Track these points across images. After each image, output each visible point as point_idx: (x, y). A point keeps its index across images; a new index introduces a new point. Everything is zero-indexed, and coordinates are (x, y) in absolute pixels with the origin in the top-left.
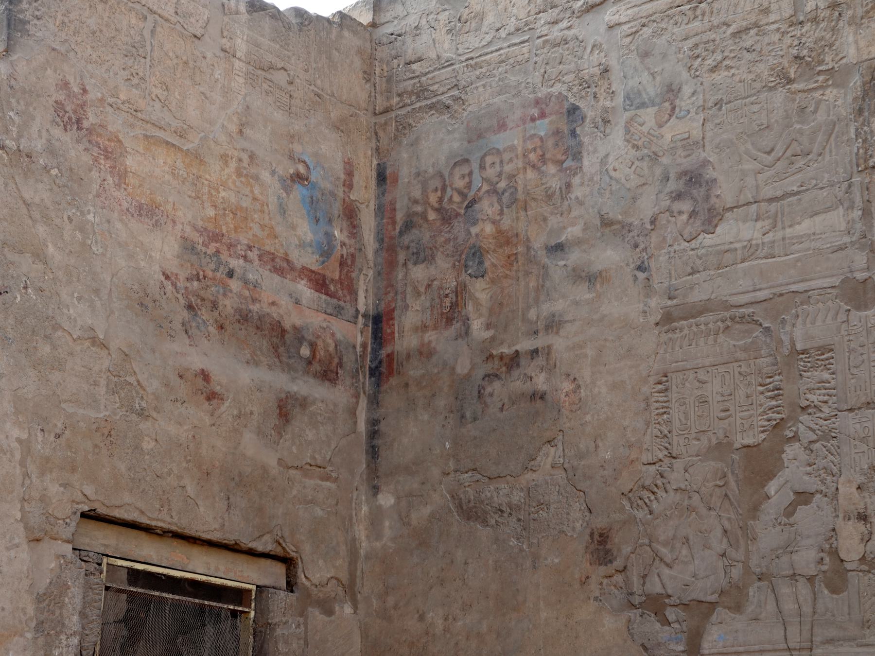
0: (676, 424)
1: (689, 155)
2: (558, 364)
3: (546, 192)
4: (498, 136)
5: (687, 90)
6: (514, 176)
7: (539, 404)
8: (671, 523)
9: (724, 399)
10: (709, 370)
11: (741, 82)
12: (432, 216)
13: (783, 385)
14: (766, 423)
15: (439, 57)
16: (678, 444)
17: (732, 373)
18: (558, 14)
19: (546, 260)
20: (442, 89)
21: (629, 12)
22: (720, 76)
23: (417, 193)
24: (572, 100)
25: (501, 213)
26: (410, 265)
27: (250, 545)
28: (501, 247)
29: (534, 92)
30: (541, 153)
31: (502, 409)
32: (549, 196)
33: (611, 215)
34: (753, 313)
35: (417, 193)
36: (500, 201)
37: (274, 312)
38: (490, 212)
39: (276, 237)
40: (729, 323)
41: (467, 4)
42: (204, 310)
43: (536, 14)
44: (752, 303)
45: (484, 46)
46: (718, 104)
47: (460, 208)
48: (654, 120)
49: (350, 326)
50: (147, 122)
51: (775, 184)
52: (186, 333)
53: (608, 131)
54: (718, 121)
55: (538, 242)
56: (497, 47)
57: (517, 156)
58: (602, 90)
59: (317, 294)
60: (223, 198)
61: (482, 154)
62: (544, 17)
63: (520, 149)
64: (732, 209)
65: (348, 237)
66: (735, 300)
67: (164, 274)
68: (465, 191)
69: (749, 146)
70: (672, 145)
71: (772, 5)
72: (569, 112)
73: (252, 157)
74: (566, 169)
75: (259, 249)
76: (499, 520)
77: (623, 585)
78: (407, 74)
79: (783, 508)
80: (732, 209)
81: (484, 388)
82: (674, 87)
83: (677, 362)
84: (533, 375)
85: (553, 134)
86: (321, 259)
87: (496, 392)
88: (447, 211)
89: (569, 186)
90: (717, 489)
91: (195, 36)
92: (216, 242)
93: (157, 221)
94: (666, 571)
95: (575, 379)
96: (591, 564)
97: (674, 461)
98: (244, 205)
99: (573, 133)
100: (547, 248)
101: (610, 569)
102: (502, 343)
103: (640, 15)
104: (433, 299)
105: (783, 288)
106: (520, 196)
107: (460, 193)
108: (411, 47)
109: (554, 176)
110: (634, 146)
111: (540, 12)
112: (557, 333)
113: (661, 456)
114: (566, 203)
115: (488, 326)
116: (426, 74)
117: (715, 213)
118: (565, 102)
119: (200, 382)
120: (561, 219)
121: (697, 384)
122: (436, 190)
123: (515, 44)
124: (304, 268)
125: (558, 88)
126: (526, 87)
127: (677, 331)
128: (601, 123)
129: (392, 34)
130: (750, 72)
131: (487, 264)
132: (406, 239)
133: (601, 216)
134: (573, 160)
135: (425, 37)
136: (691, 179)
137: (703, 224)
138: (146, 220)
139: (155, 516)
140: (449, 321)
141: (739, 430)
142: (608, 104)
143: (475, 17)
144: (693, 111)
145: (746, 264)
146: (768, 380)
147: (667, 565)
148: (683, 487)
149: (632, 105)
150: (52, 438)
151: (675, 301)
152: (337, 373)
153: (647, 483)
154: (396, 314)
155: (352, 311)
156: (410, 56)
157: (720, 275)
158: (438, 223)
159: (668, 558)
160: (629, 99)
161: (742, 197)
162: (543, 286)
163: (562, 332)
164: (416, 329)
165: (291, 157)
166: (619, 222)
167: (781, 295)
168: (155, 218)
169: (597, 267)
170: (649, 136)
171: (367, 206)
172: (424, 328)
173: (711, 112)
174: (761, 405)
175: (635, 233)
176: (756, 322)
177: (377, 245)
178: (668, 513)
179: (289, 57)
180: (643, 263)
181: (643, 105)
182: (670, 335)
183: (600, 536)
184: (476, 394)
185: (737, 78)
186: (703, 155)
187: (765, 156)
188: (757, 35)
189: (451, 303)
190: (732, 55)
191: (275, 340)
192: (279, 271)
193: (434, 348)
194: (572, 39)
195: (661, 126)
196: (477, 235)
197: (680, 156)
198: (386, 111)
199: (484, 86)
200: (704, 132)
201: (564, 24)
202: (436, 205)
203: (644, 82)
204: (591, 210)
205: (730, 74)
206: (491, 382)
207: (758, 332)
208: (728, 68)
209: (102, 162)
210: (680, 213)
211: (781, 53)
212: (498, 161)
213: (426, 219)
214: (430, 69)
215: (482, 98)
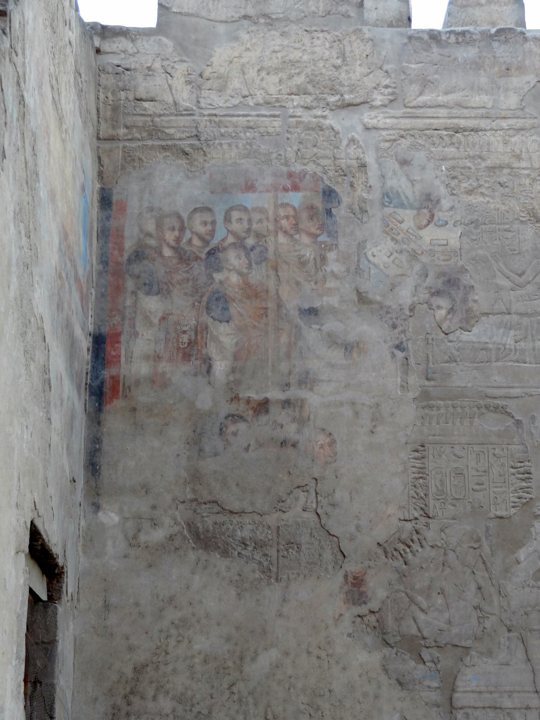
0: (433, 490)
1: (447, 260)
2: (312, 417)
3: (300, 259)
4: (245, 195)
5: (446, 203)
6: (265, 236)
7: (290, 451)
8: (427, 574)
9: (479, 474)
10: (466, 447)
11: (495, 210)
12: (167, 252)
13: (533, 470)
14: (518, 500)
15: (175, 104)
16: (435, 506)
17: (486, 453)
18: (312, 102)
19: (299, 320)
20: (178, 135)
21: (388, 121)
22: (476, 199)
23: (151, 227)
24: (328, 182)
25: (250, 266)
26: (141, 295)
28: (249, 297)
29: (286, 164)
30: (294, 222)
31: (247, 449)
32: (302, 263)
33: (370, 296)
34: (506, 405)
35: (151, 227)
36: (247, 255)
40: (483, 410)
41: (209, 63)
43: (288, 94)
44: (506, 397)
45: (228, 108)
46: (475, 223)
47: (200, 252)
48: (413, 221)
51: (526, 302)
53: (365, 219)
54: (474, 237)
55: (292, 302)
56: (245, 113)
57: (267, 219)
58: (360, 182)
61: (227, 207)
62: (297, 100)
64: (487, 314)
66: (489, 391)
68: (208, 237)
69: (503, 266)
70: (431, 248)
71: (523, 154)
72: (324, 192)
74: (321, 243)
76: (243, 552)
77: (376, 624)
78: (138, 109)
79: (531, 572)
80: (487, 314)
81: (226, 427)
82: (432, 197)
83: (434, 435)
84: (284, 423)
85: (307, 208)
87: (240, 432)
88: (185, 252)
89: (324, 259)
90: (471, 550)
94: (421, 616)
95: (330, 434)
96: (344, 603)
97: (430, 521)
99: (329, 212)
100: (300, 309)
101: (363, 610)
102: (249, 388)
103: (399, 127)
104: (168, 333)
105: (533, 390)
106: (270, 254)
108: (143, 88)
109: (307, 246)
110: (393, 239)
111: (292, 94)
112: (311, 389)
113: (416, 515)
114: (320, 274)
115: (233, 370)
116: (160, 115)
117: (472, 315)
118: (320, 183)
120: (315, 287)
121: (454, 457)
122: (173, 229)
123: (265, 116)
125: (311, 168)
126: (277, 158)
127: (435, 409)
128: (358, 211)
129: (118, 66)
130: (504, 204)
132: (136, 268)
133: (359, 293)
134: (329, 236)
135: (160, 80)
136: (449, 281)
137: (461, 321)
140: (187, 357)
141: (492, 502)
142: (365, 195)
143: (218, 78)
144: (451, 223)
145: (500, 364)
146: (519, 465)
147: (422, 610)
148: (440, 545)
149: (390, 203)
151: (433, 383)
153: (404, 536)
154: (123, 338)
156: (141, 92)
157: (477, 368)
158: (175, 261)
159: (424, 605)
160: (388, 197)
161: (496, 306)
162: (295, 344)
163: (315, 388)
164: (147, 358)
166: (378, 303)
167: (532, 395)
169: (352, 338)
170: (408, 234)
172: (158, 358)
173: (467, 228)
174: (512, 484)
175: (394, 315)
176: (509, 414)
177: (101, 267)
178: (424, 566)
180: (401, 343)
181: (402, 206)
182: (427, 411)
183: (354, 579)
184: (217, 430)
185: (492, 206)
186: (460, 263)
187: (517, 277)
188: (509, 174)
189: (190, 340)
190: (487, 185)
193: (169, 379)
194: (327, 128)
195: (420, 228)
196: (221, 282)
197: (438, 258)
198: (112, 139)
199: (230, 145)
200: (461, 243)
201: (319, 112)
202: (173, 244)
203: (404, 186)
204: (347, 285)
205: (485, 201)
206: (234, 422)
207: (510, 422)
208: (482, 194)
210: (439, 307)
211: (532, 196)
212: (245, 217)
213: (161, 254)
214: (165, 111)
215: (224, 156)
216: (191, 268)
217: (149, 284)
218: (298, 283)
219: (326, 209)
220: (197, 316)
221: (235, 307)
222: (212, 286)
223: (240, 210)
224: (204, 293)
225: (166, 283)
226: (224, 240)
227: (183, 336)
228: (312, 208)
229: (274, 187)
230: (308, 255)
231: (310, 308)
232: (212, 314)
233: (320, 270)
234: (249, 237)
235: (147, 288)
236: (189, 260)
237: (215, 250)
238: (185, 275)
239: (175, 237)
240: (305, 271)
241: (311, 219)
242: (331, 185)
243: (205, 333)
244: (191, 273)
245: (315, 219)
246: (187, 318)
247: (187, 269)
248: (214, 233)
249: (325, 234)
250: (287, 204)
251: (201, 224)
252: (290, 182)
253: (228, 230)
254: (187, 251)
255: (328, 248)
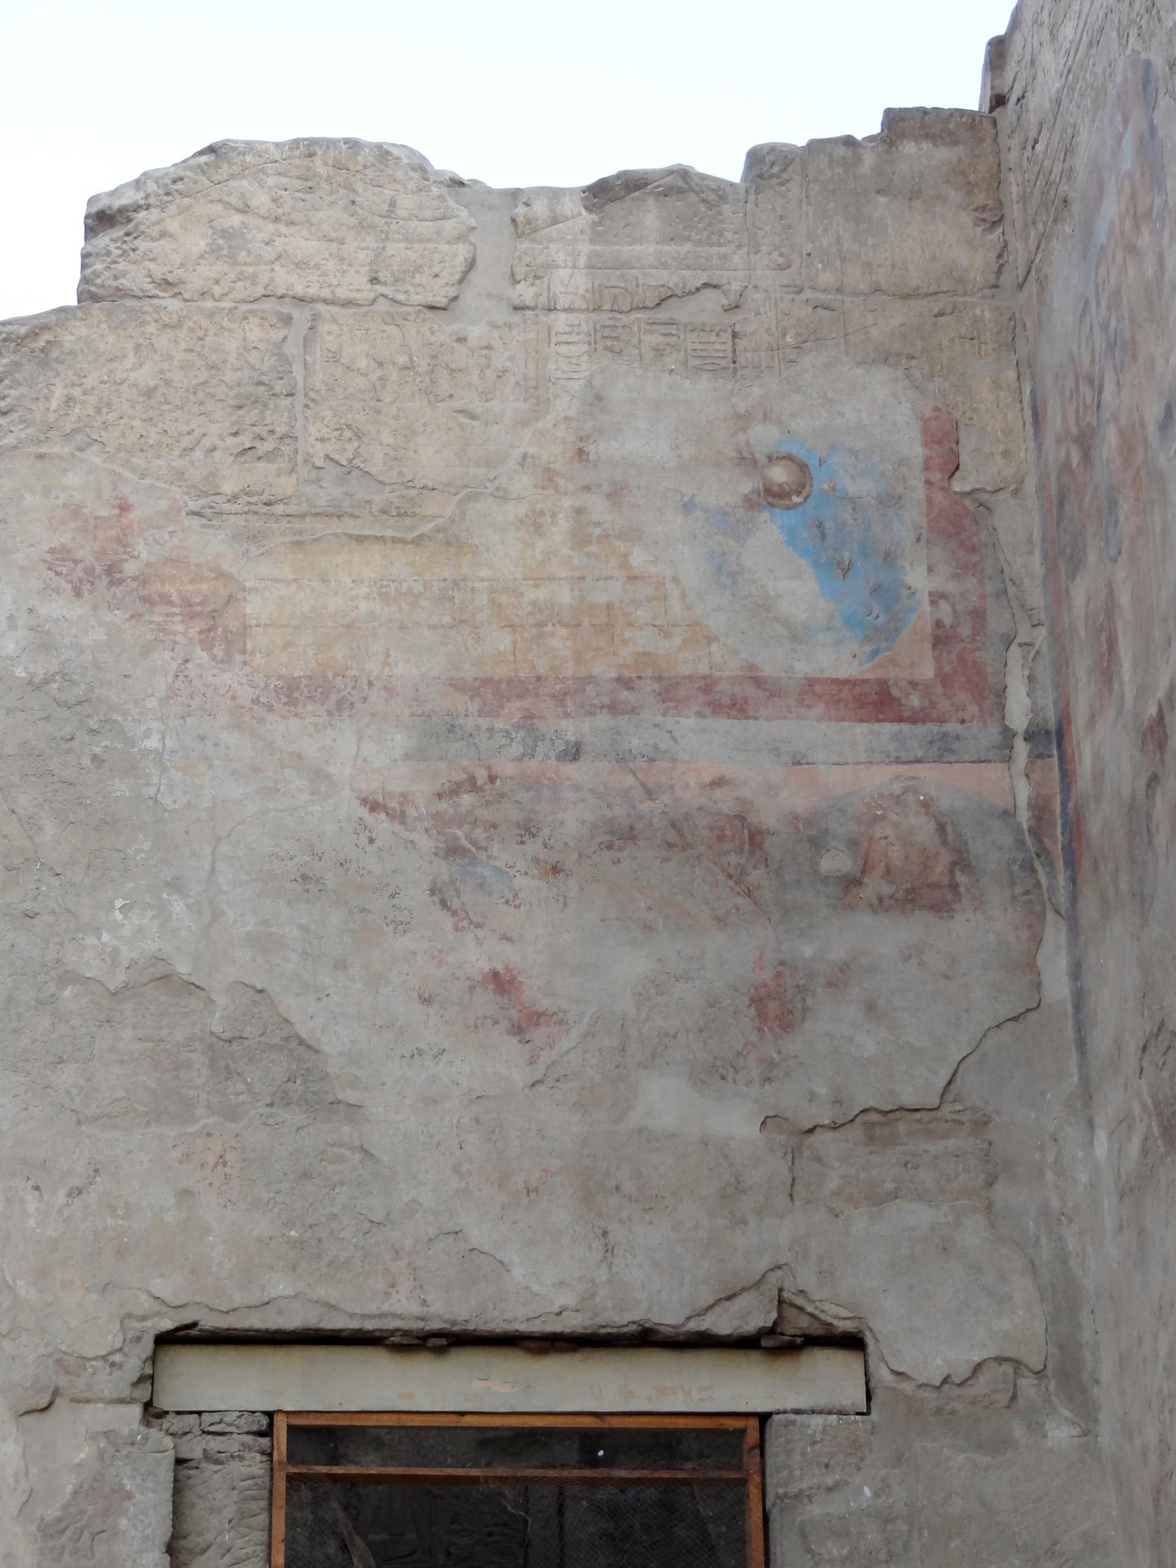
27: (692, 1326)
37: (725, 800)
39: (710, 639)
42: (495, 848)
49: (994, 772)
50: (302, 516)
52: (444, 904)
59: (861, 730)
60: (534, 603)
65: (956, 577)
67: (364, 802)
73: (616, 494)
75: (659, 678)
86: (868, 648)
91: (432, 308)
92: (520, 697)
93: (340, 704)
98: (601, 599)
119: (486, 1001)
124: (811, 682)
138: (310, 707)
139: (372, 1308)
150: (61, 1198)
152: (954, 886)
155: (993, 735)
165: (746, 461)
168: (333, 698)
171: (1016, 492)
179: (724, 257)
191: (734, 859)
192: (737, 708)
209: (180, 628)
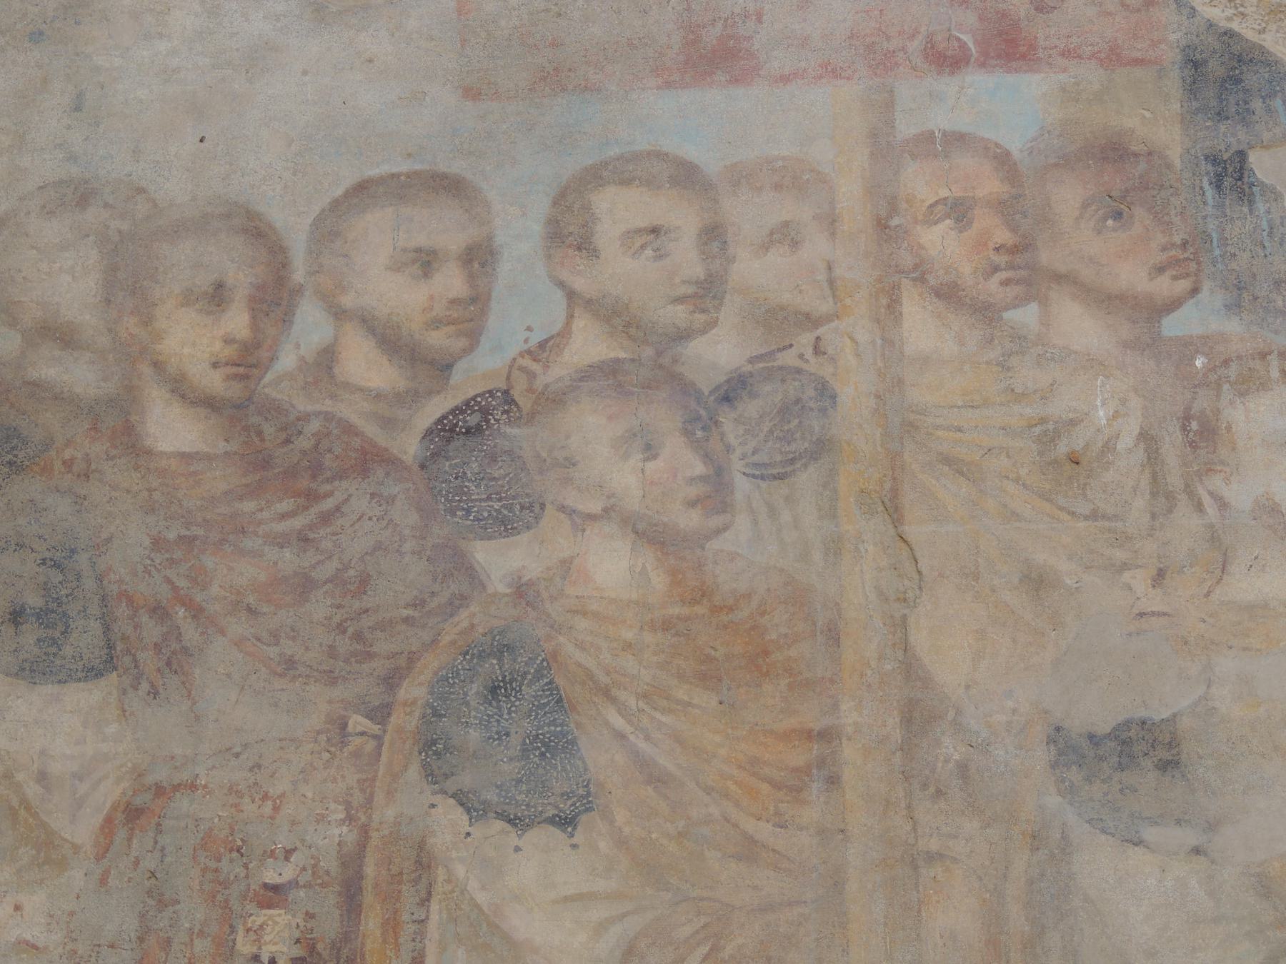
6: (810, 321)
12: (172, 429)
19: (1053, 801)
25: (715, 494)
28: (708, 675)
30: (1003, 236)
38: (626, 479)
57: (831, 222)
63: (849, 191)
68: (438, 339)
72: (1194, 64)
74: (1189, 346)
89: (1204, 435)
99: (1231, 174)
107: (391, 341)
120: (1154, 601)
122: (217, 296)
131: (600, 758)
134: (1234, 307)
196: (522, 591)
202: (214, 382)
212: (684, 219)
213: (130, 441)
216: (326, 518)
217: (42, 616)
218: (1037, 582)
219: (1214, 159)
220: (358, 798)
221: (621, 736)
222: (463, 618)
223: (650, 183)
224: (412, 659)
225: (159, 612)
226: (543, 350)
227: (259, 917)
228: (1113, 151)
229: (870, 48)
230: (1101, 415)
231: (1128, 724)
232: (465, 780)
233: (1183, 497)
234: (714, 324)
235: (30, 635)
236: (316, 470)
237: (486, 412)
238: (289, 560)
239: (228, 341)
240: (1084, 508)
241: (1118, 215)
242: (1235, 26)
243: (409, 897)
244: (327, 545)
245: (1140, 214)
246: (288, 810)
247: (298, 522)
248: (483, 313)
249: (1211, 297)
250: (957, 140)
251: (396, 267)
252: (971, 18)
253: (571, 295)
254: (305, 418)
255: (1233, 371)
